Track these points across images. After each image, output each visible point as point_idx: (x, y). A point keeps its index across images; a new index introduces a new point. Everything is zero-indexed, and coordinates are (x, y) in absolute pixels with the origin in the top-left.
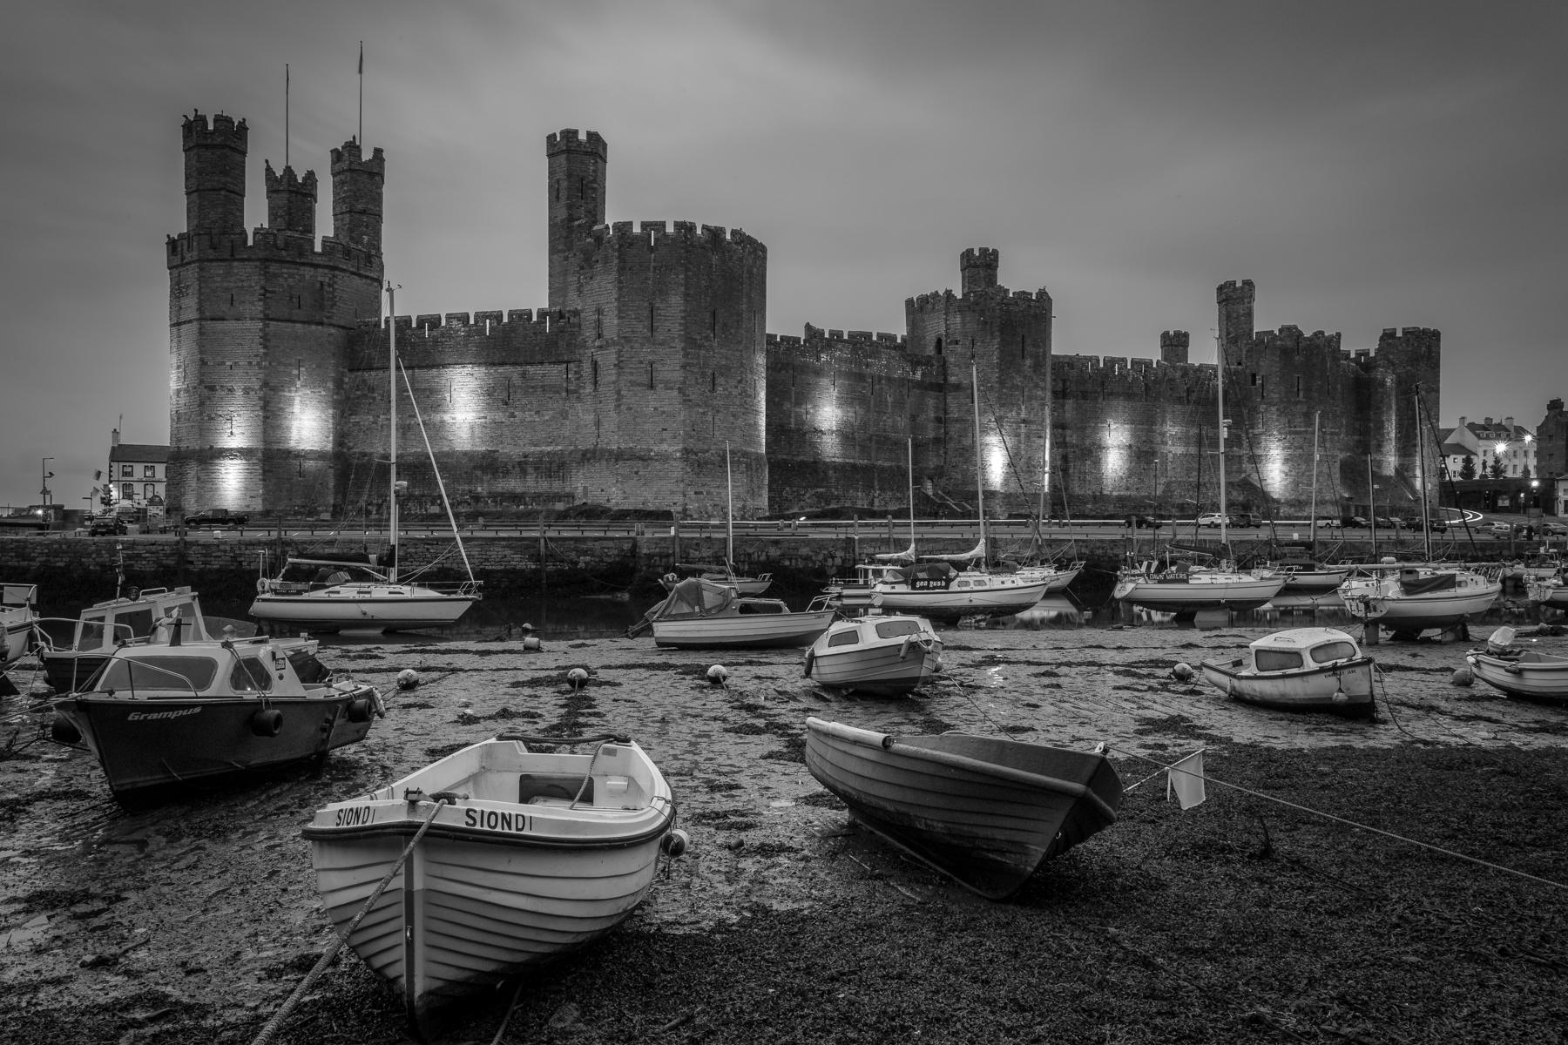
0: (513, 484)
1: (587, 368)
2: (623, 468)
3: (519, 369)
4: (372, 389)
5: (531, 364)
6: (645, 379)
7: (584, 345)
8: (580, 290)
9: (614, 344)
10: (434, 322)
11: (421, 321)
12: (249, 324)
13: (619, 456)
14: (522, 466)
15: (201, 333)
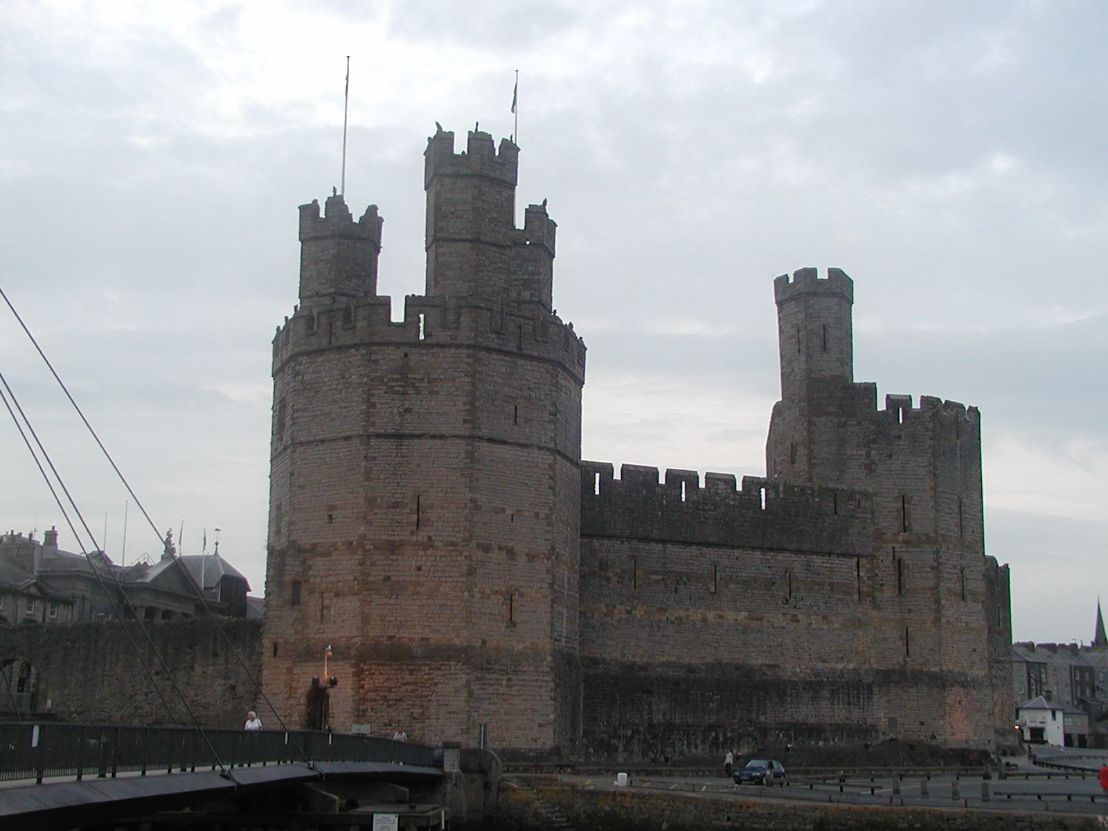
0: (804, 712)
1: (886, 570)
2: (954, 695)
3: (803, 558)
4: (604, 566)
5: (817, 553)
6: (958, 590)
7: (879, 536)
8: (869, 467)
9: (929, 540)
10: (692, 478)
11: (674, 477)
12: (536, 454)
13: (940, 682)
14: (813, 687)
15: (470, 455)
